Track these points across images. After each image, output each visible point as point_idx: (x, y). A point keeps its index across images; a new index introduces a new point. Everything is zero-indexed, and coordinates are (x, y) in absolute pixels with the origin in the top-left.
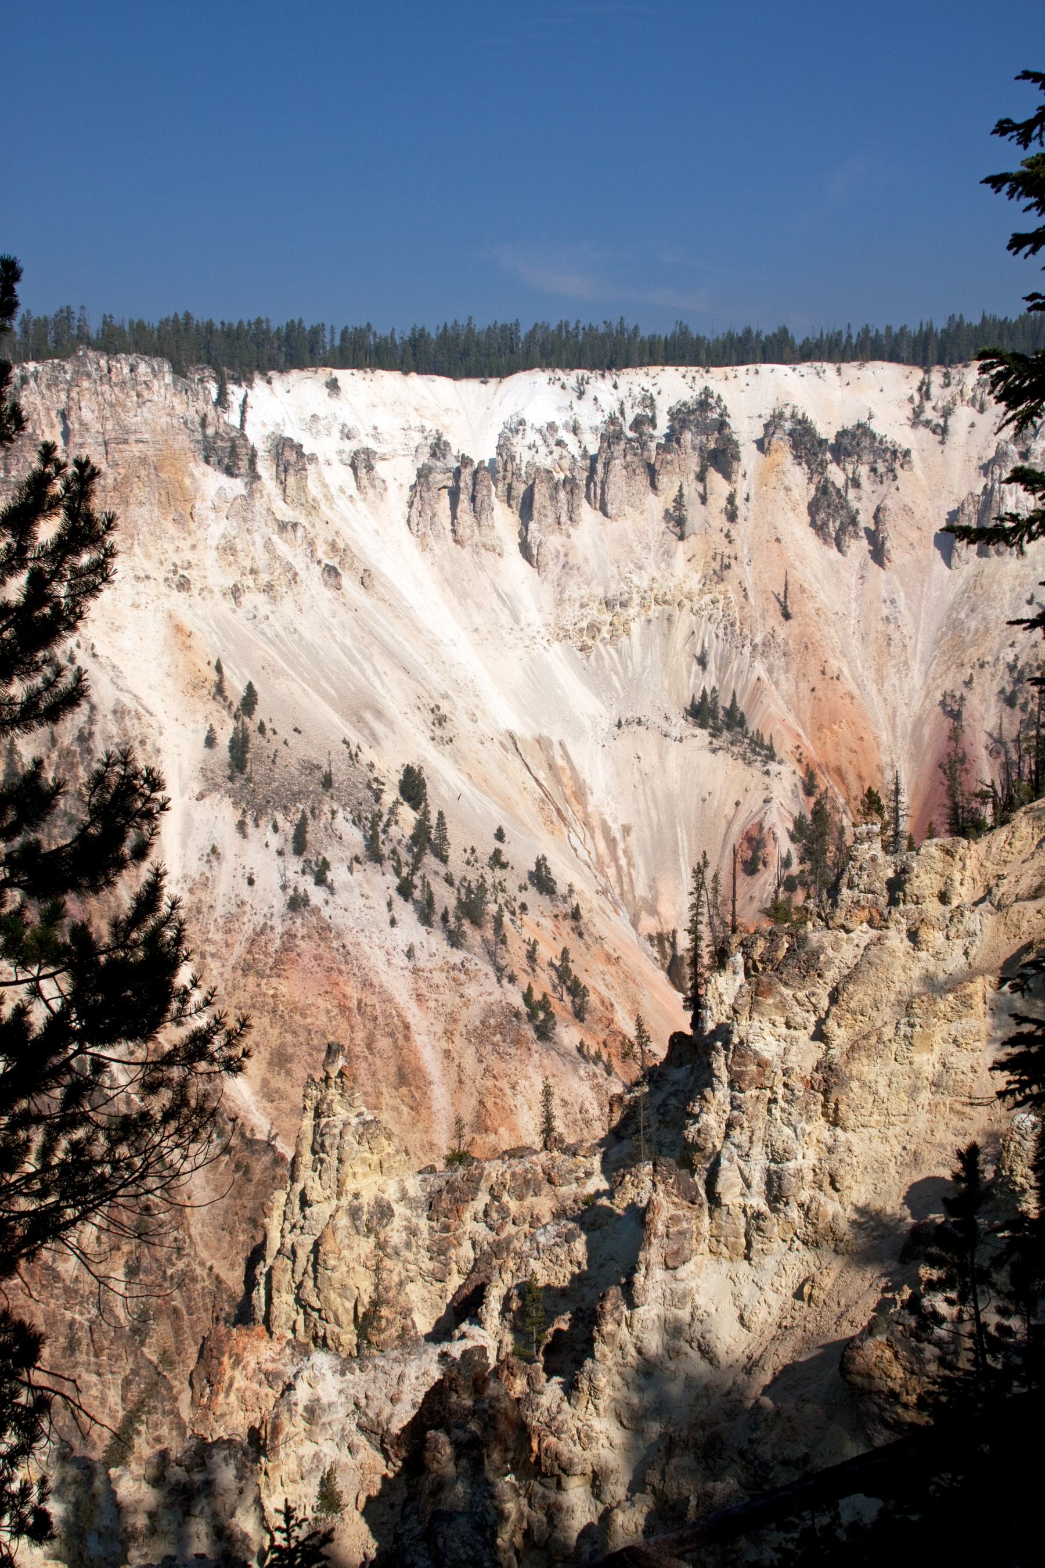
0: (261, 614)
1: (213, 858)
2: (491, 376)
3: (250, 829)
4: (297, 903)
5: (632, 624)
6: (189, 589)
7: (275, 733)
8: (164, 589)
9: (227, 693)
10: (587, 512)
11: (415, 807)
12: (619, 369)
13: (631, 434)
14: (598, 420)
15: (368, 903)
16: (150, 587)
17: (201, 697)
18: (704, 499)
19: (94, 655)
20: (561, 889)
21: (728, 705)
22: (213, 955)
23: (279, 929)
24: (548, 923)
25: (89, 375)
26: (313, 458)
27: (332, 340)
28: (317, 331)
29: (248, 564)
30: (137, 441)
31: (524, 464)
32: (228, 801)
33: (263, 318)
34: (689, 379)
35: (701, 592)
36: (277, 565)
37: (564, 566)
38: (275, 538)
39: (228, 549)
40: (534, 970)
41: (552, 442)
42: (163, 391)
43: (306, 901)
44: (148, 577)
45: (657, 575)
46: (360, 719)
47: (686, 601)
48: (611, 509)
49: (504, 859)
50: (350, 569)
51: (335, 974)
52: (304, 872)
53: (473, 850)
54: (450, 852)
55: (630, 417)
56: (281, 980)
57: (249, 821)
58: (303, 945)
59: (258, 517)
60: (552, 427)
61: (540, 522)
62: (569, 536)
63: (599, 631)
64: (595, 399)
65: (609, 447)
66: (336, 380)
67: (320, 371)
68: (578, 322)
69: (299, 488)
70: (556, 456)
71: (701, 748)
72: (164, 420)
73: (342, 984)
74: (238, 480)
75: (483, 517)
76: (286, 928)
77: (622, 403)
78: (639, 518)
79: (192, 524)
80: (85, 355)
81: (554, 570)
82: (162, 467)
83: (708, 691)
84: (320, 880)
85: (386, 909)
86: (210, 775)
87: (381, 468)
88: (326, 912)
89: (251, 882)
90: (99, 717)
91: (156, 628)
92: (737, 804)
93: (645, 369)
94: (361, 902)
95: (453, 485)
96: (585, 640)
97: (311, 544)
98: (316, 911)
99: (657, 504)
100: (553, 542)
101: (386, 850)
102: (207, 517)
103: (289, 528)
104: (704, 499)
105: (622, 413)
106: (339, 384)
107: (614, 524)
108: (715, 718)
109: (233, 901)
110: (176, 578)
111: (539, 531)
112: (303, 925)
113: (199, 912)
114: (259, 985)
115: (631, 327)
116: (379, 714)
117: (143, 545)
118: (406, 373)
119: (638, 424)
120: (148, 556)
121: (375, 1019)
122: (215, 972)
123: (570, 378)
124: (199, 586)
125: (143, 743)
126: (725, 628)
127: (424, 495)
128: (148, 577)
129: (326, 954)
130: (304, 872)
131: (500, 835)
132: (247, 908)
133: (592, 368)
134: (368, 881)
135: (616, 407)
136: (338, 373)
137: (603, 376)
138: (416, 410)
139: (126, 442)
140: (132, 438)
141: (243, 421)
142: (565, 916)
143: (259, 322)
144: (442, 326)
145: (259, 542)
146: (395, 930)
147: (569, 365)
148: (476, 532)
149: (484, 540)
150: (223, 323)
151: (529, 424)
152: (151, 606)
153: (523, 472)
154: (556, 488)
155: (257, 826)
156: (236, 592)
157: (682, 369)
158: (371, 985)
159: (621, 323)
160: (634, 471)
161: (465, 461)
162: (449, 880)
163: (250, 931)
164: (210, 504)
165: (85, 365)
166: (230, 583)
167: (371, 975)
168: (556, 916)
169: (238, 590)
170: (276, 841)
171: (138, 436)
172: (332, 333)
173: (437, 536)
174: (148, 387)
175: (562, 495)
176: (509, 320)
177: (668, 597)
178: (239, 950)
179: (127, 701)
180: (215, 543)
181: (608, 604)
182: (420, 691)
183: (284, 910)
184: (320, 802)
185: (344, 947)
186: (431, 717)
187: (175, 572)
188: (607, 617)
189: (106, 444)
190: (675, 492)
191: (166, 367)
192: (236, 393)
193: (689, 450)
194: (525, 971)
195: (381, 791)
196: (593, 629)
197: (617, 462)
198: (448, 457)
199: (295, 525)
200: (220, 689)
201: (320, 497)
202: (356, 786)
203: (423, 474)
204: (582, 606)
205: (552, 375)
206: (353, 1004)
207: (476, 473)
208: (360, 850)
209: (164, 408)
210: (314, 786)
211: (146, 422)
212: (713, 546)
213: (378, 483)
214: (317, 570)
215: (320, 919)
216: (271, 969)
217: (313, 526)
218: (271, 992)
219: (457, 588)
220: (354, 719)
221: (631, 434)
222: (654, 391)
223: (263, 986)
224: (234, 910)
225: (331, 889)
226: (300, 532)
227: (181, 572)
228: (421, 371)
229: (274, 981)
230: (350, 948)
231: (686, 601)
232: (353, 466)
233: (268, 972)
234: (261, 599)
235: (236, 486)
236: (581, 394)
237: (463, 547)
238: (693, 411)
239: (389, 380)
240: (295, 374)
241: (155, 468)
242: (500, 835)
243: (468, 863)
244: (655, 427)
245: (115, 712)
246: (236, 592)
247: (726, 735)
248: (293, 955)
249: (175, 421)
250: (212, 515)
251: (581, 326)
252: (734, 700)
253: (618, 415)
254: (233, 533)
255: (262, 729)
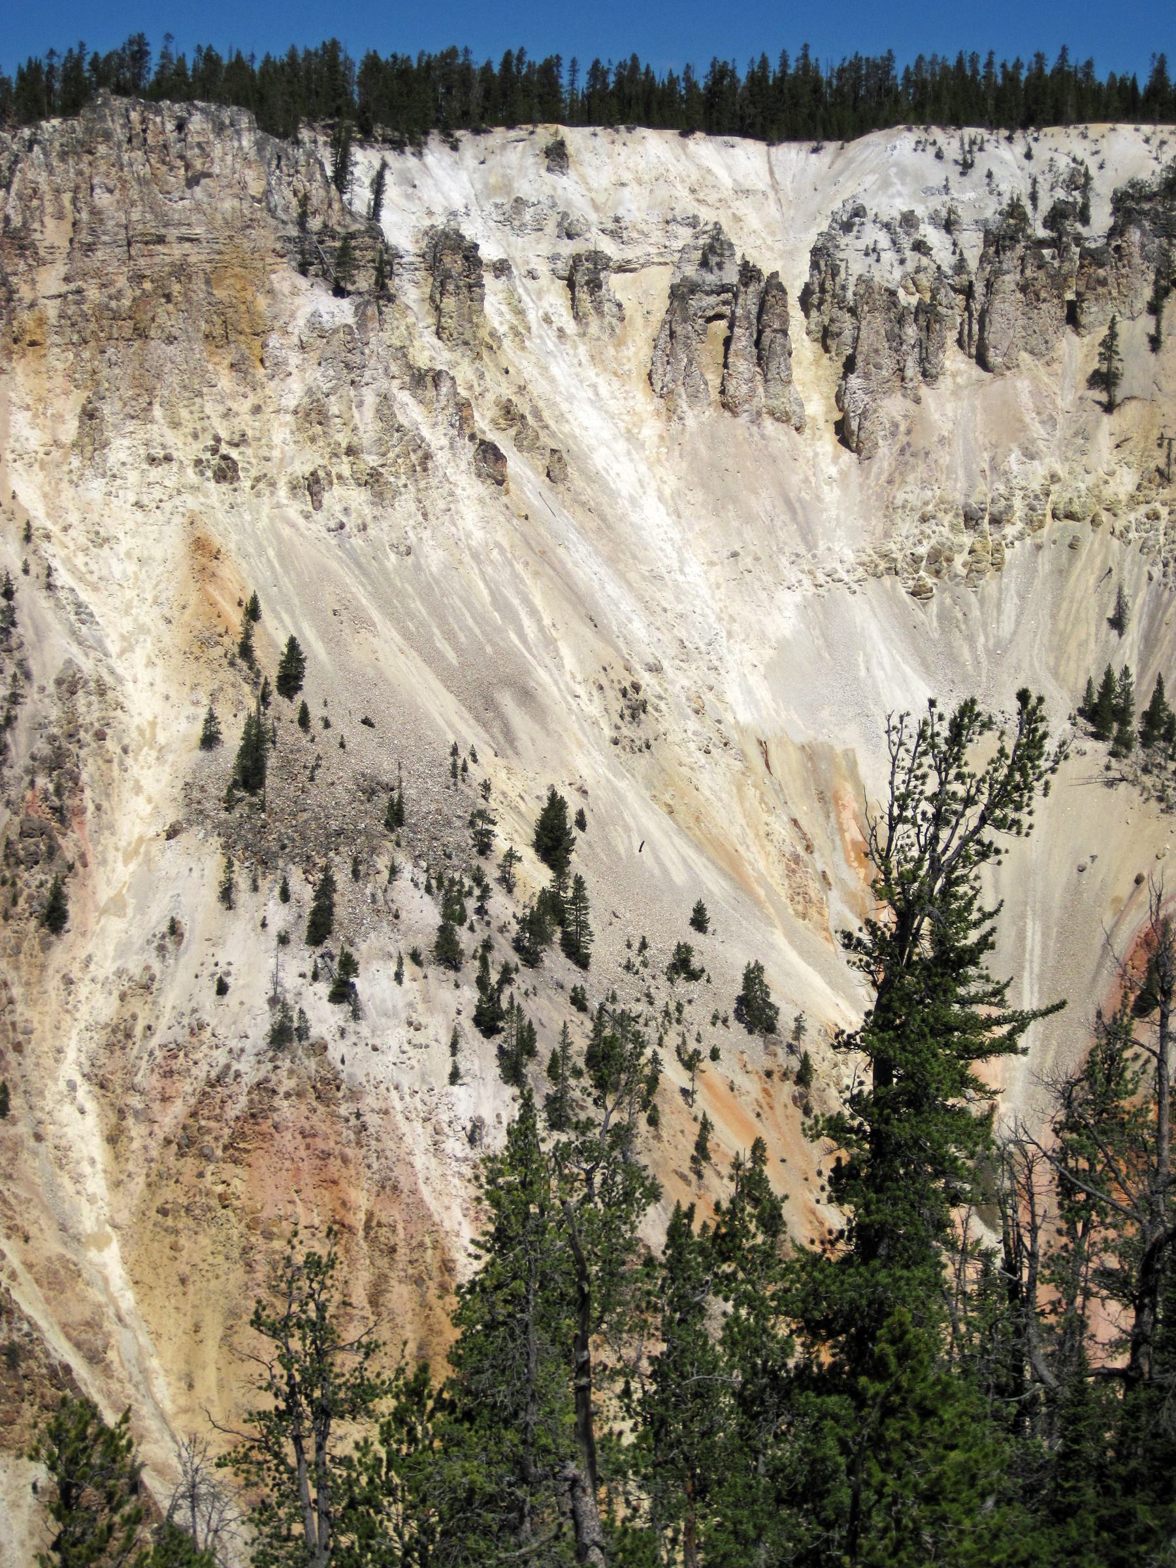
0: (351, 524)
1: (169, 942)
2: (830, 139)
3: (242, 895)
4: (285, 1035)
5: (1008, 553)
6: (235, 478)
7: (327, 725)
8: (191, 475)
9: (258, 653)
10: (954, 362)
11: (552, 867)
12: (1038, 129)
13: (1042, 233)
14: (991, 211)
15: (419, 1038)
16: (165, 475)
17: (209, 662)
18: (1155, 343)
19: (50, 587)
20: (785, 1022)
21: (1146, 706)
22: (136, 1114)
23: (250, 1079)
24: (751, 1086)
25: (107, 136)
26: (501, 268)
27: (572, 83)
28: (550, 69)
29: (343, 439)
30: (182, 239)
31: (852, 280)
32: (216, 842)
33: (460, 48)
34: (1155, 142)
35: (1133, 502)
36: (394, 441)
37: (902, 451)
38: (404, 397)
39: (313, 415)
40: (700, 1175)
41: (906, 243)
42: (229, 158)
43: (303, 1033)
44: (168, 459)
45: (1061, 470)
46: (490, 704)
47: (1105, 516)
48: (994, 358)
49: (696, 963)
50: (530, 449)
51: (335, 1165)
52: (315, 977)
53: (644, 945)
54: (592, 949)
55: (1046, 204)
56: (238, 1170)
57: (242, 880)
58: (286, 1110)
59: (372, 362)
60: (909, 220)
61: (866, 376)
62: (917, 401)
63: (949, 560)
64: (990, 175)
65: (997, 252)
66: (561, 144)
67: (540, 129)
68: (991, 54)
69: (460, 315)
70: (910, 266)
71: (1088, 781)
72: (228, 204)
73: (343, 1184)
74: (346, 304)
75: (773, 366)
76: (261, 1075)
77: (1035, 182)
78: (1042, 371)
79: (261, 372)
80: (105, 103)
81: (885, 454)
82: (221, 279)
83: (1117, 675)
84: (343, 993)
85: (447, 1051)
86: (196, 794)
87: (615, 283)
88: (335, 1051)
89: (222, 989)
90: (31, 693)
91: (168, 543)
92: (1138, 880)
93: (1082, 127)
94: (404, 1033)
95: (725, 313)
96: (924, 576)
97: (463, 408)
98: (321, 1048)
99: (1077, 352)
100: (893, 406)
101: (468, 941)
102: (285, 362)
103: (429, 379)
104: (1155, 343)
105: (1034, 197)
106: (570, 149)
107: (999, 384)
108: (1125, 722)
109: (185, 1021)
110: (215, 461)
111: (867, 392)
112: (291, 1072)
113: (128, 1036)
114: (201, 1175)
115: (1082, 63)
116: (527, 696)
117: (167, 405)
118: (685, 133)
119: (1055, 218)
120: (175, 425)
121: (393, 1250)
122: (136, 1145)
123: (951, 141)
124: (254, 473)
125: (100, 736)
126: (1166, 565)
127: (679, 329)
128: (168, 459)
129: (323, 1128)
130: (315, 977)
131: (699, 921)
132: (206, 1035)
133: (993, 125)
134: (426, 1000)
135: (1025, 189)
136: (565, 132)
137: (1009, 139)
138: (693, 191)
139: (161, 240)
140: (172, 233)
141: (378, 205)
142: (785, 1076)
143: (452, 53)
144: (758, 60)
145: (370, 398)
146: (455, 1089)
147: (956, 121)
148: (761, 390)
149: (775, 403)
150: (394, 56)
151: (871, 214)
152: (167, 506)
153: (849, 295)
154: (900, 321)
155: (255, 888)
156: (313, 486)
157: (1147, 129)
158: (395, 1188)
159: (1063, 57)
160: (1037, 295)
161: (749, 273)
162: (578, 1001)
163: (203, 1075)
164: (296, 340)
165: (102, 119)
166: (307, 469)
167: (398, 1171)
168: (769, 1074)
169: (317, 481)
170: (279, 916)
171: (184, 230)
172: (574, 69)
173: (694, 397)
174: (205, 154)
175: (911, 332)
176: (873, 51)
177: (1076, 508)
178: (178, 1109)
179: (87, 665)
180: (291, 402)
181: (971, 519)
182: (608, 655)
183: (263, 1044)
184: (373, 850)
185: (358, 1115)
186: (618, 704)
187: (215, 451)
188: (967, 539)
189: (129, 244)
190: (1104, 331)
191: (244, 121)
192: (364, 161)
193: (1137, 260)
194: (683, 1177)
195: (490, 832)
196: (938, 560)
197: (1007, 278)
198: (727, 266)
199: (437, 377)
200: (246, 651)
201: (502, 329)
202: (449, 823)
203: (680, 293)
204: (924, 519)
205: (923, 136)
206: (358, 1220)
207: (766, 292)
208: (426, 940)
209: (230, 186)
210: (372, 818)
211: (198, 208)
212: (1160, 421)
213: (607, 307)
214: (468, 450)
215: (324, 1063)
216: (225, 1148)
217: (481, 376)
218: (220, 1188)
219: (714, 487)
220: (479, 704)
221: (1042, 233)
222: (1092, 164)
223: (209, 1178)
224: (182, 1036)
225: (356, 1015)
226: (445, 389)
227: (224, 449)
228: (714, 128)
229: (229, 1170)
230: (372, 1119)
231: (1105, 516)
232: (571, 285)
233: (219, 1153)
234: (358, 497)
235: (341, 311)
236: (966, 166)
237: (735, 414)
238: (1150, 198)
239: (654, 147)
240: (500, 134)
241: (208, 282)
242: (699, 921)
243: (628, 967)
244: (1085, 219)
245: (59, 682)
246: (313, 486)
247: (1138, 753)
248: (266, 1126)
249: (245, 205)
250: (294, 359)
251: (998, 61)
252: (1159, 692)
253: (1026, 203)
254: (325, 388)
255: (304, 720)
